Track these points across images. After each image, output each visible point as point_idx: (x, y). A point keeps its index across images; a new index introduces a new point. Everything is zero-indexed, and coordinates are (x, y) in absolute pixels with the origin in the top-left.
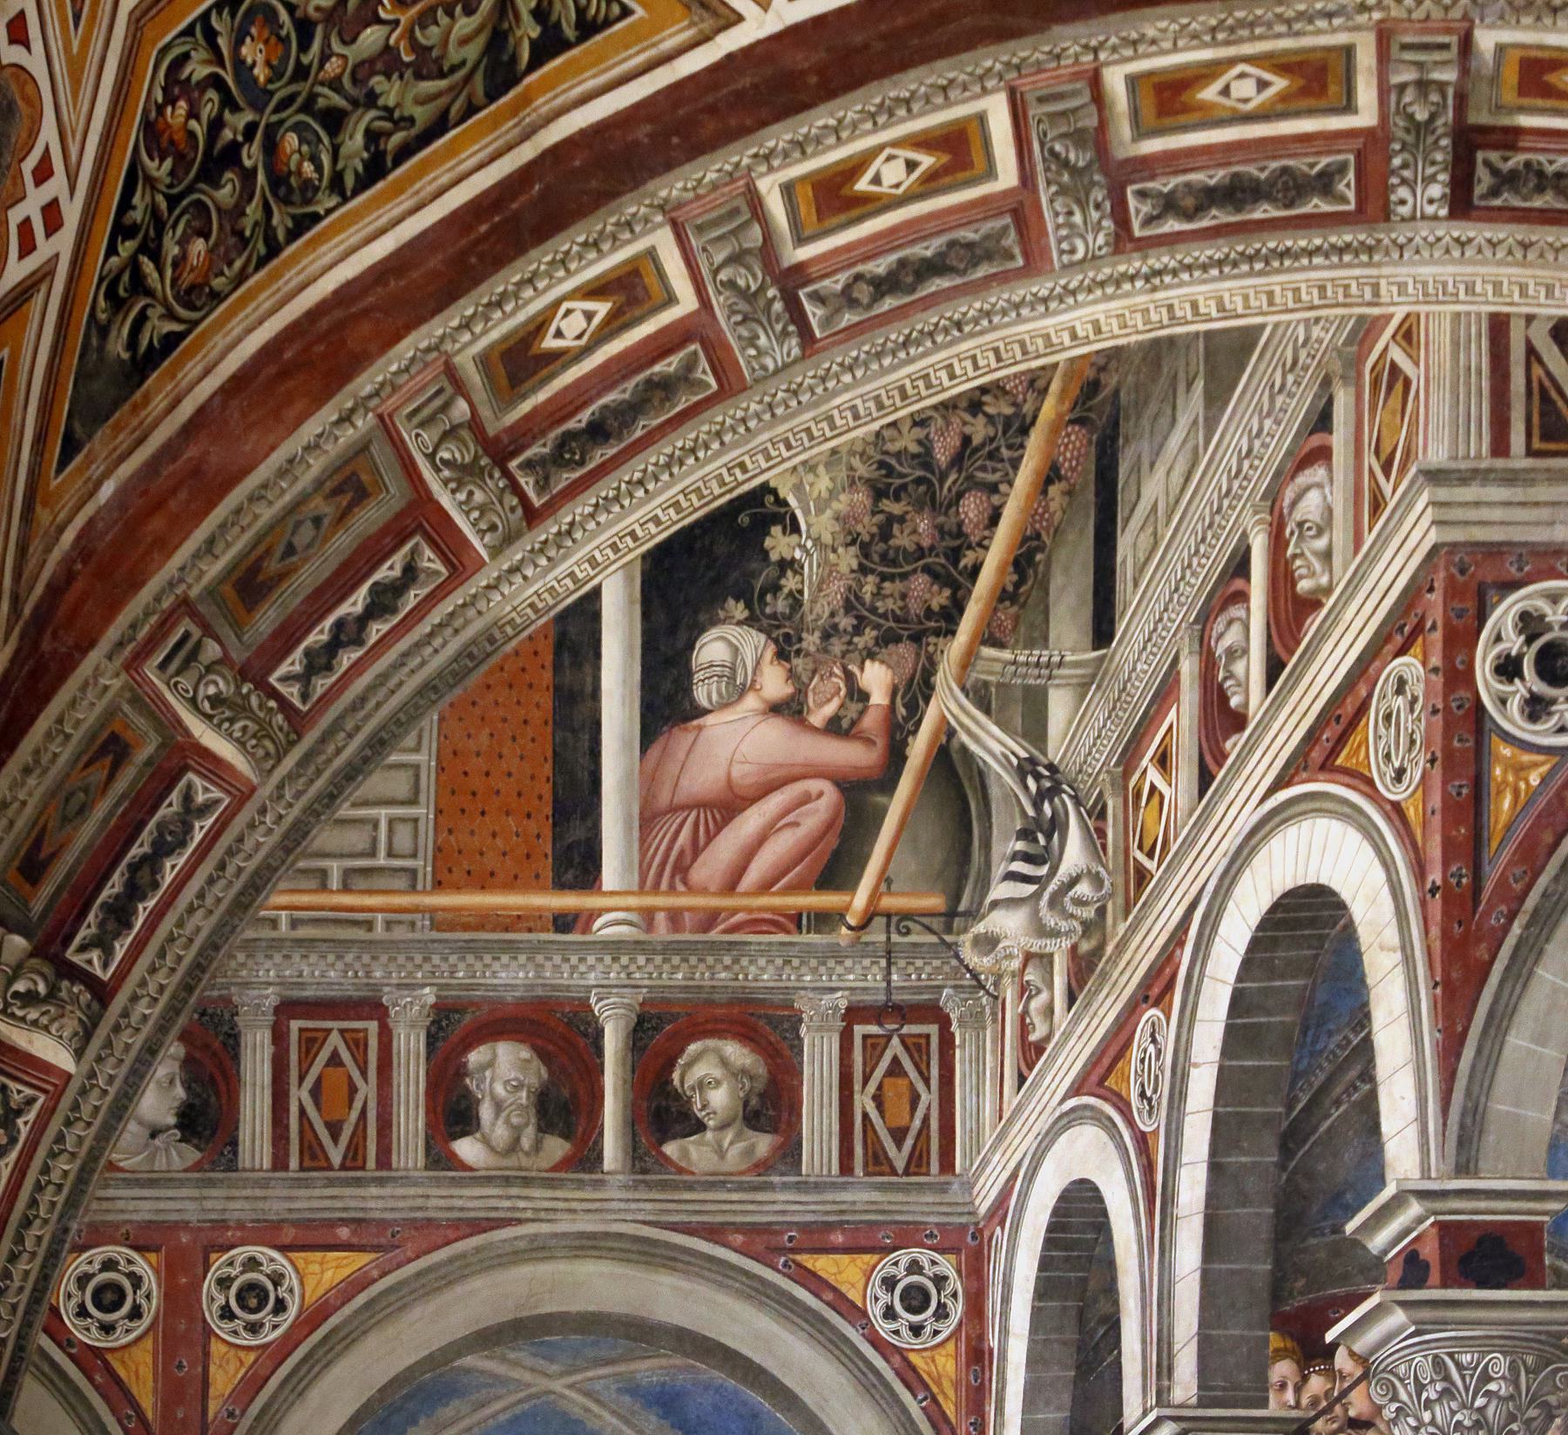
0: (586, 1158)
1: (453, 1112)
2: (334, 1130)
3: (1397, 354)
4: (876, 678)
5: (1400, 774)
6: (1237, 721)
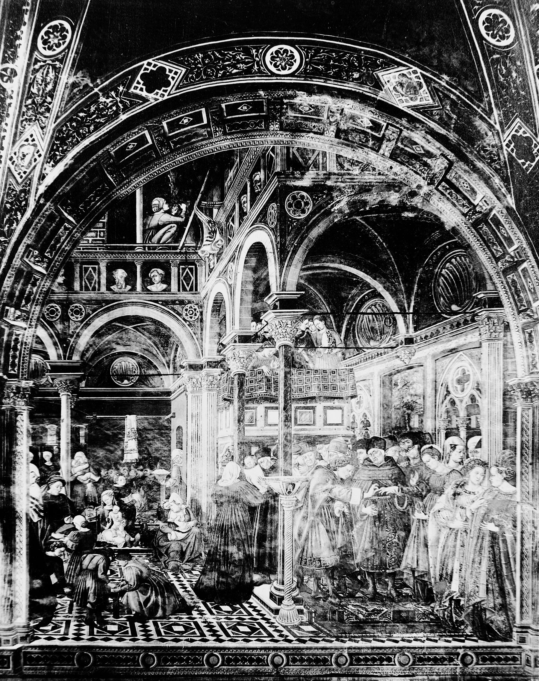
0: (134, 289)
1: (111, 281)
2: (91, 283)
3: (271, 153)
4: (183, 206)
5: (273, 223)
6: (246, 214)
